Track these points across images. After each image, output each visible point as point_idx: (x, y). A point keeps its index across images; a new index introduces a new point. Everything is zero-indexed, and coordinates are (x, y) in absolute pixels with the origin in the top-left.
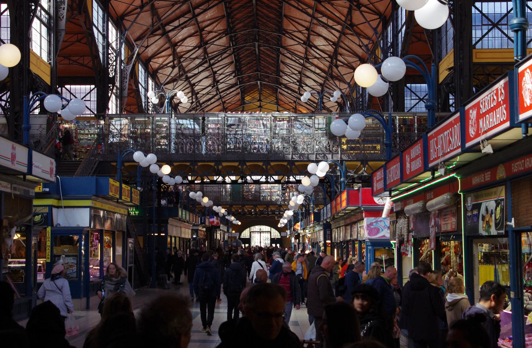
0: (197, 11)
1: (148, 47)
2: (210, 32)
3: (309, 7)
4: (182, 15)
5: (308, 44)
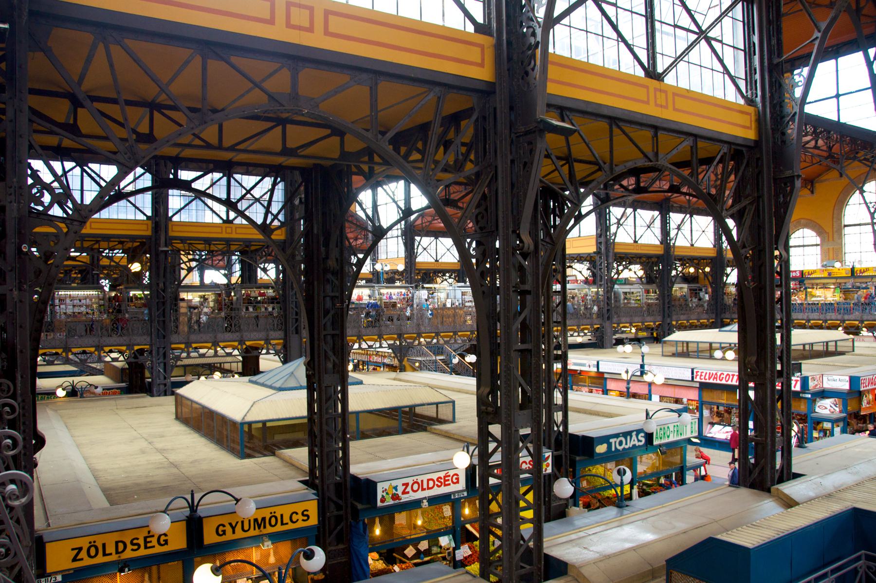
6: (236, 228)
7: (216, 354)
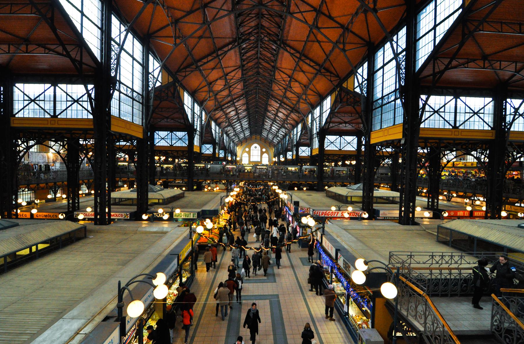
0: (235, 101)
2: (240, 110)
3: (279, 100)
5: (276, 115)
7: (182, 183)
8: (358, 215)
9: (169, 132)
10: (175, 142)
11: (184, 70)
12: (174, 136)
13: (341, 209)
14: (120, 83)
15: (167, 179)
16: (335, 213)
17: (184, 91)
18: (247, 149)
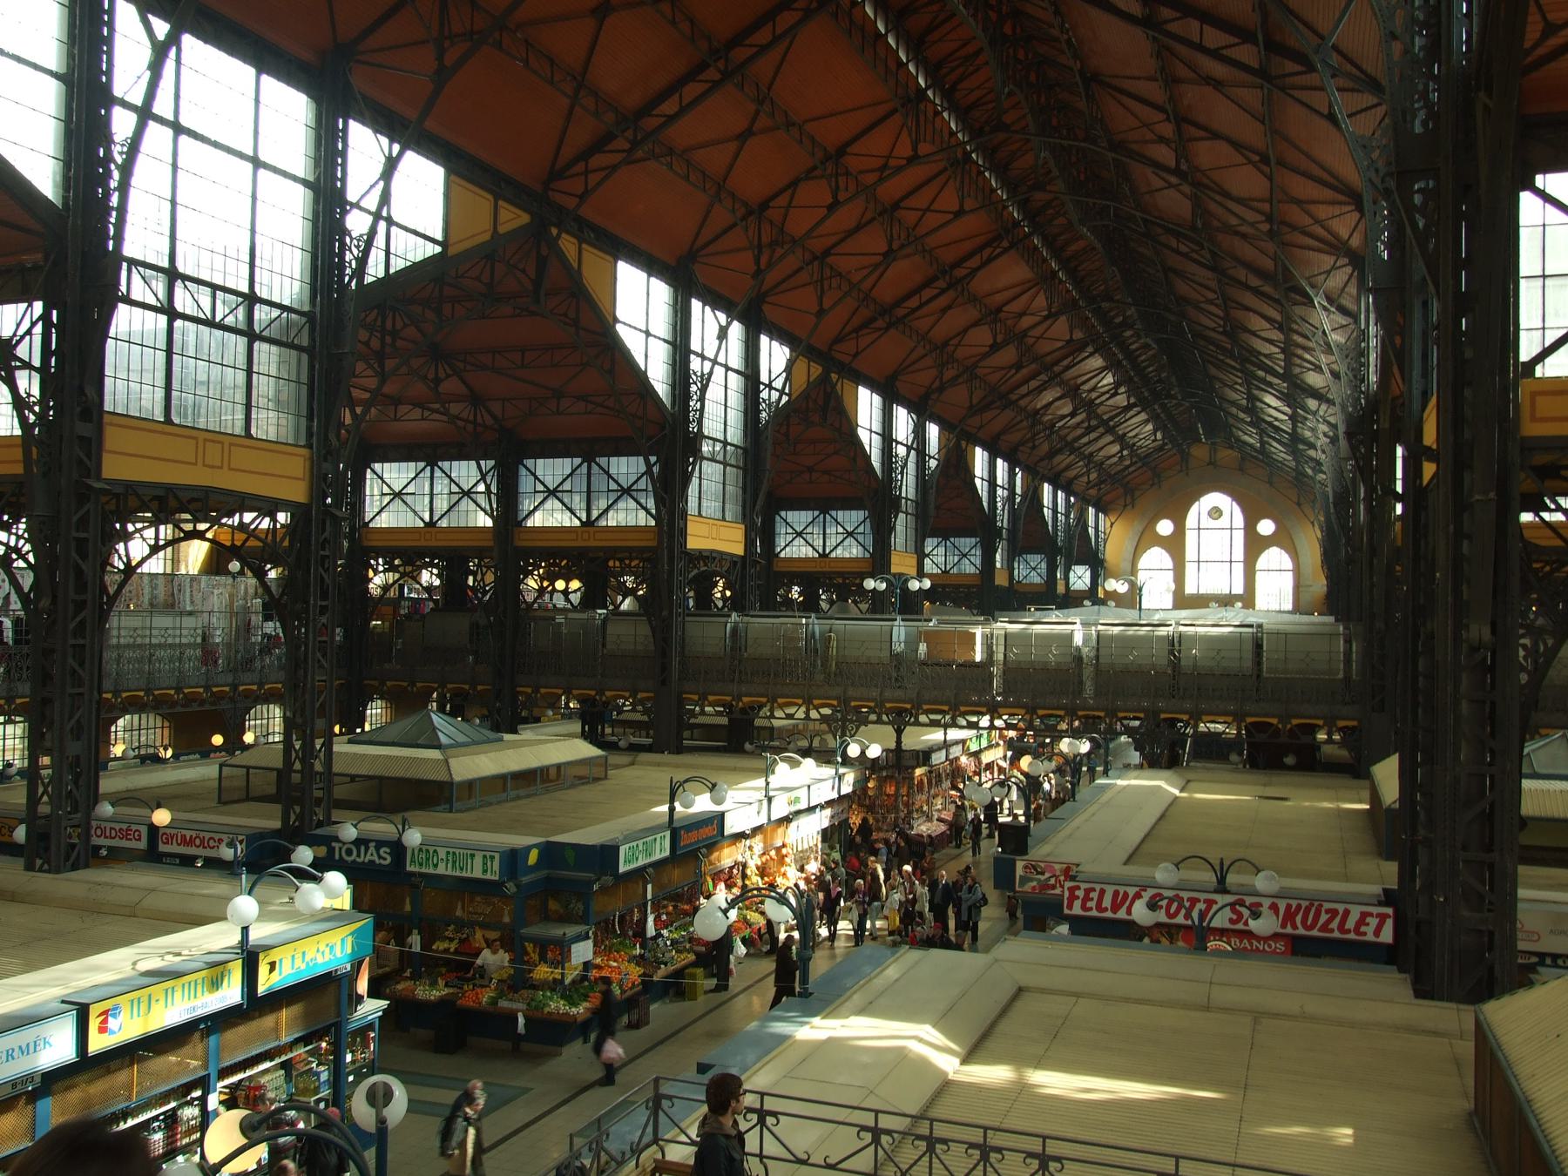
1: (857, 353)
2: (1022, 314)
4: (927, 284)
6: (594, 532)
8: (1188, 916)
9: (578, 461)
10: (603, 504)
11: (580, 167)
12: (599, 482)
13: (1231, 879)
14: (173, 275)
15: (601, 692)
16: (1194, 901)
17: (616, 259)
18: (1165, 527)
